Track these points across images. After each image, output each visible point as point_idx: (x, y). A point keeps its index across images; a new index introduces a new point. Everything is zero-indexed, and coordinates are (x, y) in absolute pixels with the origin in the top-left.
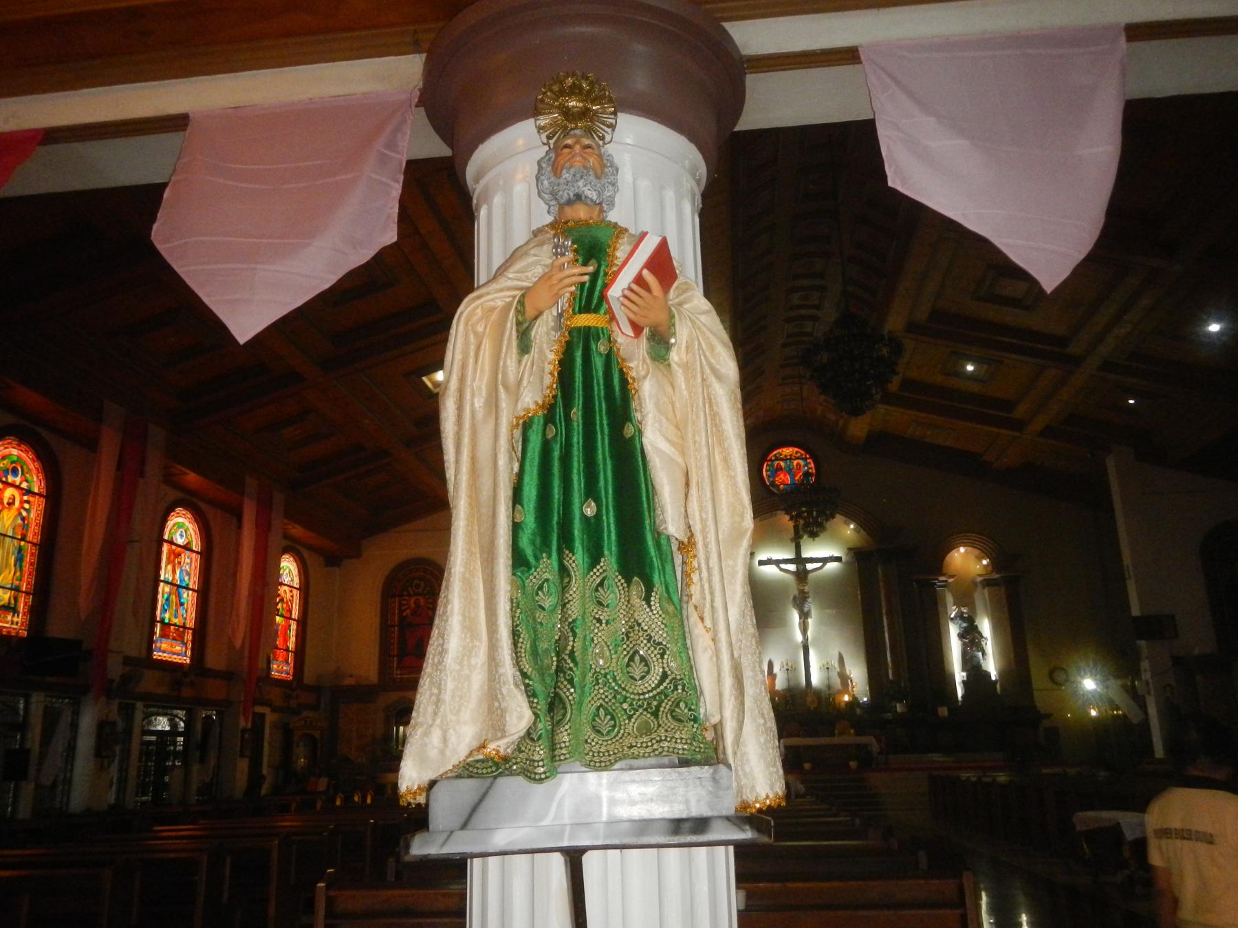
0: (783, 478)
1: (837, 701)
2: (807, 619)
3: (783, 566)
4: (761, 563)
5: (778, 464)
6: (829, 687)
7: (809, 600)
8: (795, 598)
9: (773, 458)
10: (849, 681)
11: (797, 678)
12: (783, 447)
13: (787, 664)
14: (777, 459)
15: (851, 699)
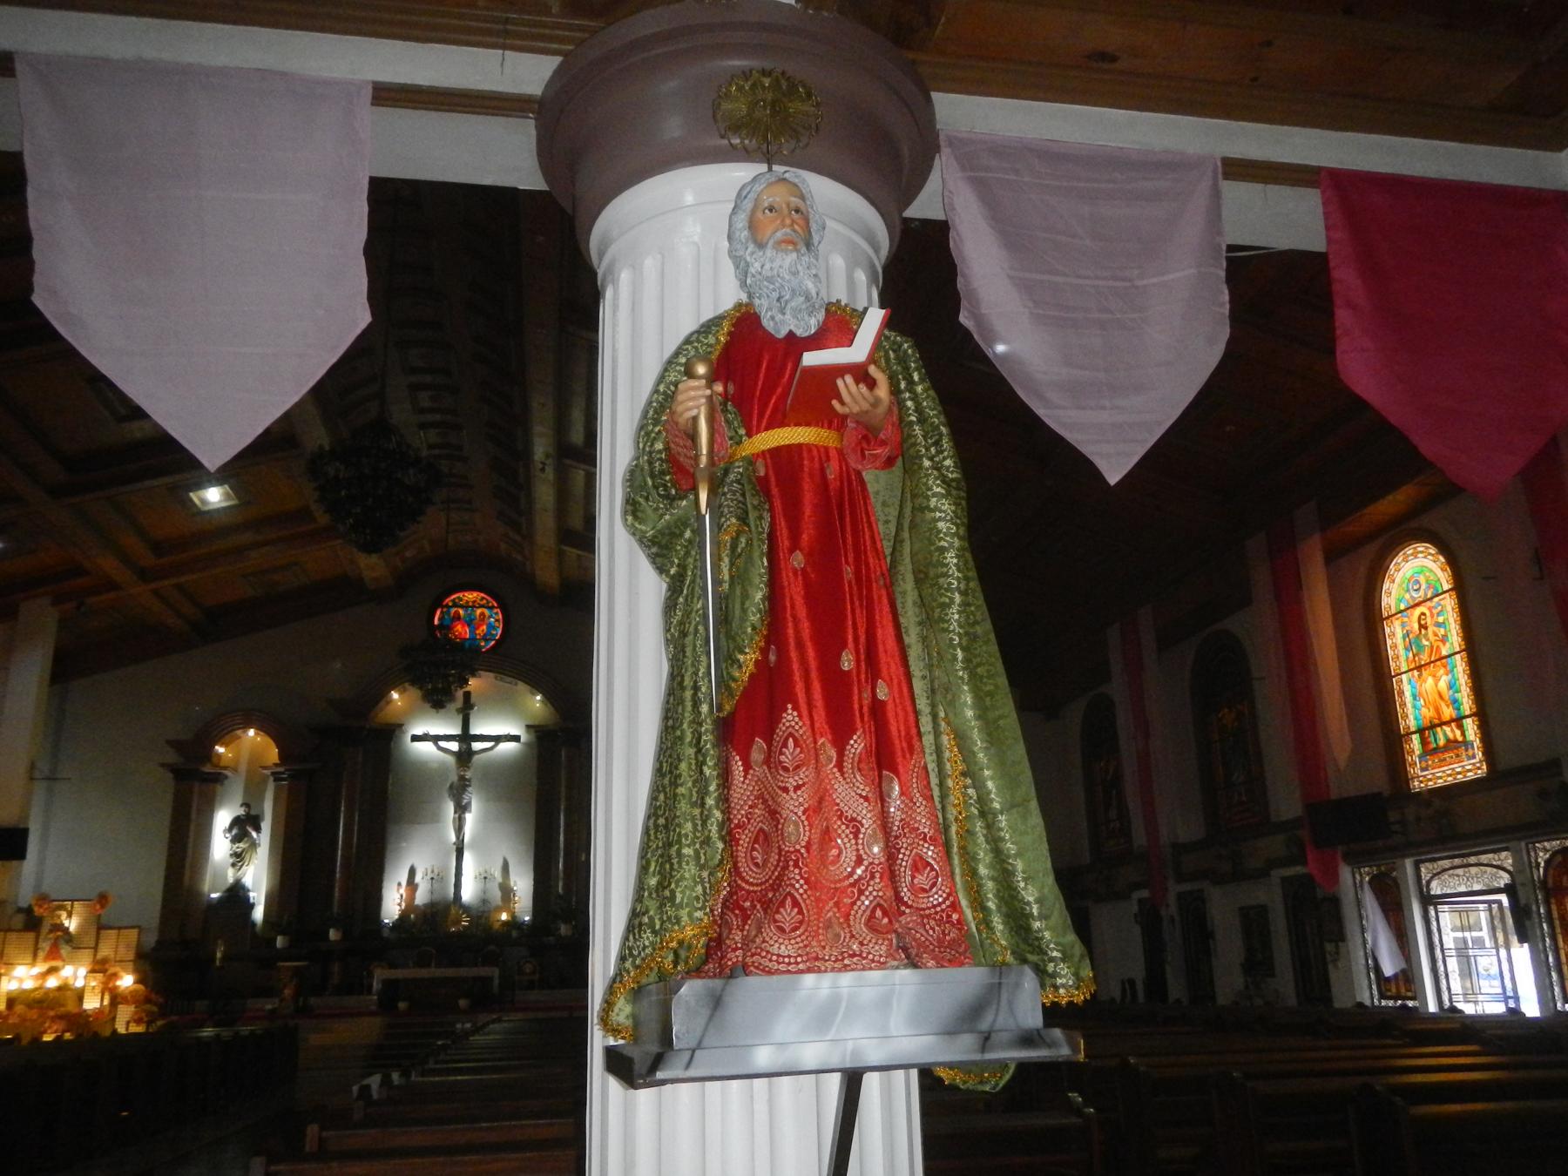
0: (460, 630)
1: (491, 920)
2: (464, 813)
3: (442, 744)
4: (415, 738)
5: (456, 611)
6: (484, 901)
7: (470, 789)
8: (451, 787)
9: (450, 604)
13: (433, 872)
14: (455, 605)
15: (510, 918)
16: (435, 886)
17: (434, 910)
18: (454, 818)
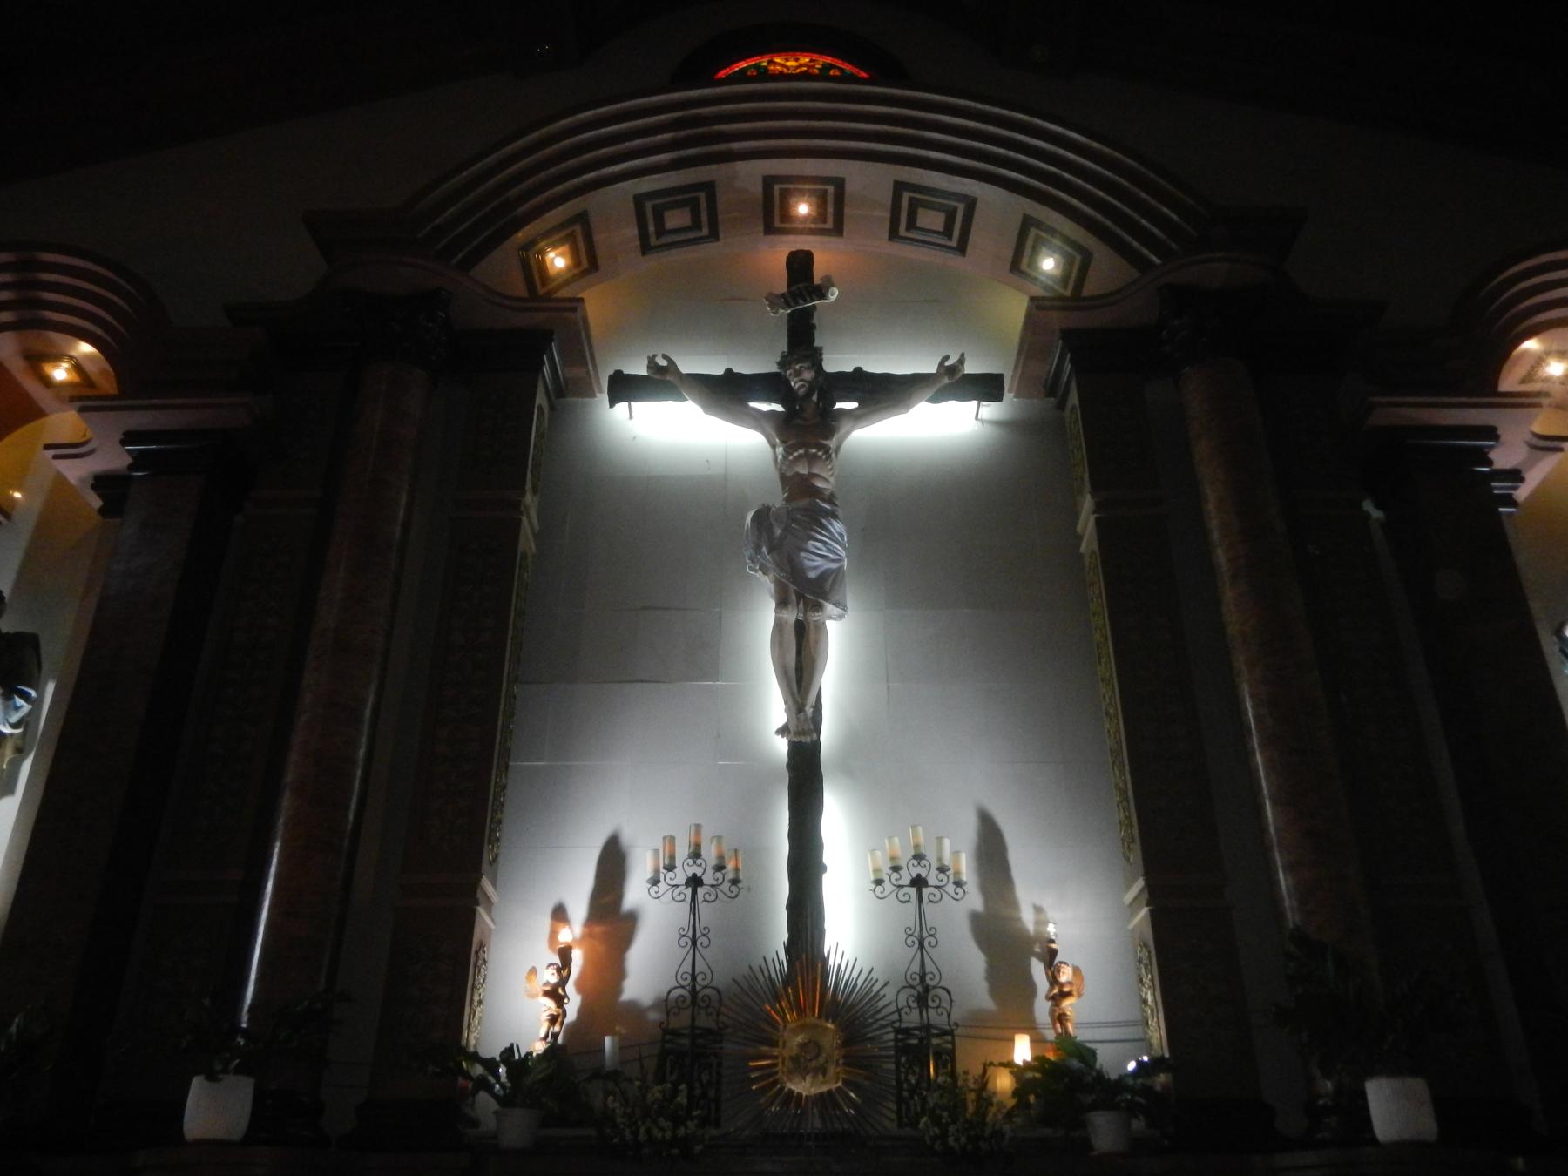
2: (818, 607)
6: (923, 991)
7: (837, 527)
10: (1038, 970)
11: (748, 926)
12: (780, 51)
13: (696, 855)
16: (703, 908)
17: (704, 1021)
18: (779, 626)
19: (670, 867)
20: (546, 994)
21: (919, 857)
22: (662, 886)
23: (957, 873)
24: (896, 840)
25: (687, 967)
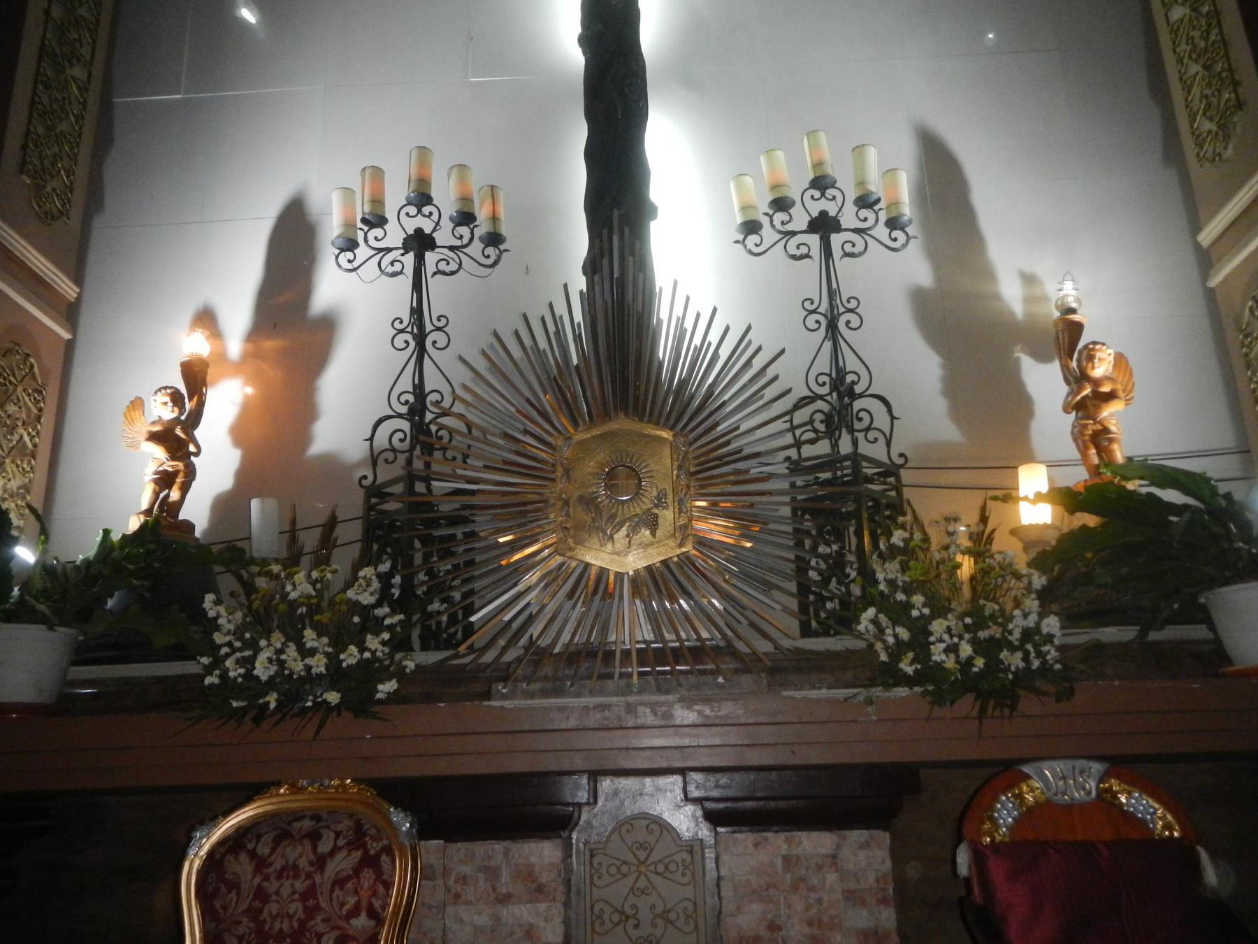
13: (422, 199)
16: (436, 287)
19: (376, 220)
20: (154, 437)
21: (821, 183)
22: (362, 252)
23: (895, 204)
24: (780, 155)
25: (406, 383)
